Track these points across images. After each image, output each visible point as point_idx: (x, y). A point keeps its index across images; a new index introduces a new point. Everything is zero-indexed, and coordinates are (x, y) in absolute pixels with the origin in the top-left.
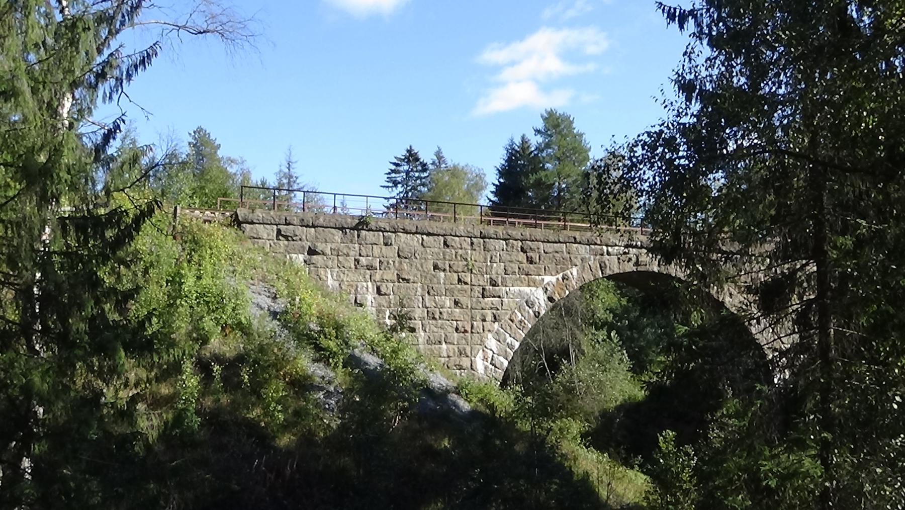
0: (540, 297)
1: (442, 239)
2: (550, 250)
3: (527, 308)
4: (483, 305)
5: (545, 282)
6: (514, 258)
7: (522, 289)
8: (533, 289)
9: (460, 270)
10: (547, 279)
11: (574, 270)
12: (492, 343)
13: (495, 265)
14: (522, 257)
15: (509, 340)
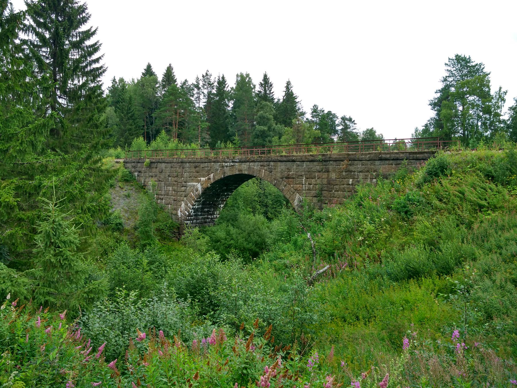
0: (199, 186)
1: (170, 165)
2: (203, 166)
3: (195, 191)
4: (181, 190)
5: (202, 180)
6: (191, 170)
7: (194, 183)
8: (197, 183)
9: (174, 176)
10: (203, 179)
11: (212, 175)
12: (183, 205)
13: (185, 174)
14: (194, 170)
15: (189, 204)
